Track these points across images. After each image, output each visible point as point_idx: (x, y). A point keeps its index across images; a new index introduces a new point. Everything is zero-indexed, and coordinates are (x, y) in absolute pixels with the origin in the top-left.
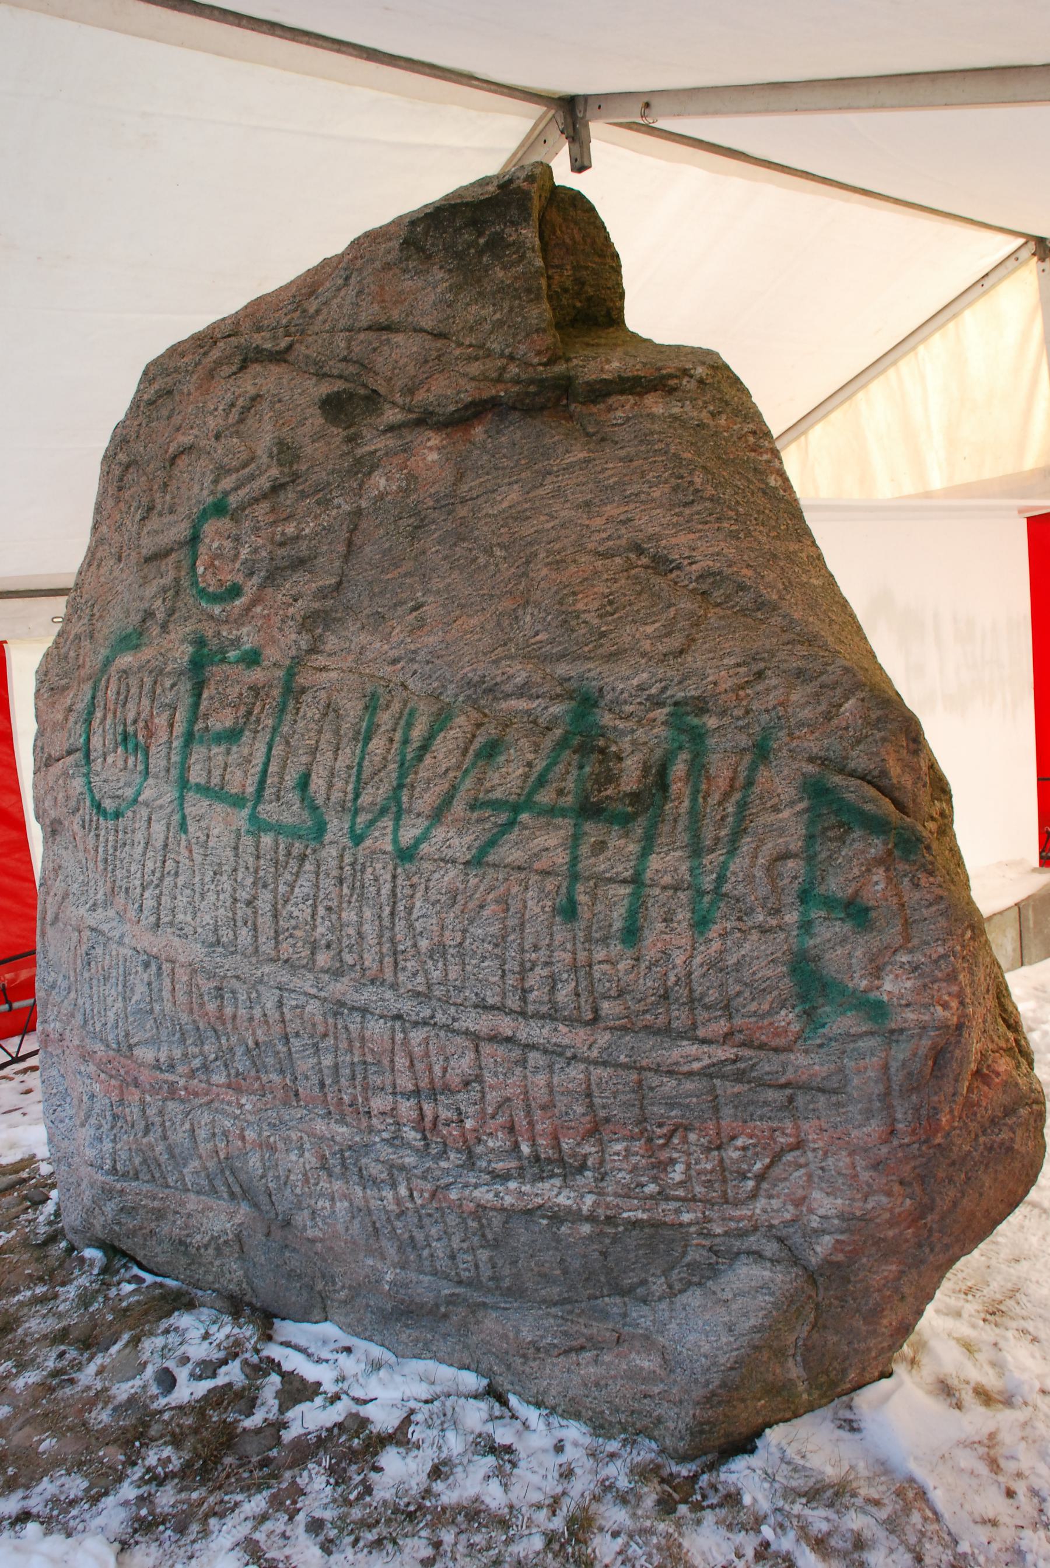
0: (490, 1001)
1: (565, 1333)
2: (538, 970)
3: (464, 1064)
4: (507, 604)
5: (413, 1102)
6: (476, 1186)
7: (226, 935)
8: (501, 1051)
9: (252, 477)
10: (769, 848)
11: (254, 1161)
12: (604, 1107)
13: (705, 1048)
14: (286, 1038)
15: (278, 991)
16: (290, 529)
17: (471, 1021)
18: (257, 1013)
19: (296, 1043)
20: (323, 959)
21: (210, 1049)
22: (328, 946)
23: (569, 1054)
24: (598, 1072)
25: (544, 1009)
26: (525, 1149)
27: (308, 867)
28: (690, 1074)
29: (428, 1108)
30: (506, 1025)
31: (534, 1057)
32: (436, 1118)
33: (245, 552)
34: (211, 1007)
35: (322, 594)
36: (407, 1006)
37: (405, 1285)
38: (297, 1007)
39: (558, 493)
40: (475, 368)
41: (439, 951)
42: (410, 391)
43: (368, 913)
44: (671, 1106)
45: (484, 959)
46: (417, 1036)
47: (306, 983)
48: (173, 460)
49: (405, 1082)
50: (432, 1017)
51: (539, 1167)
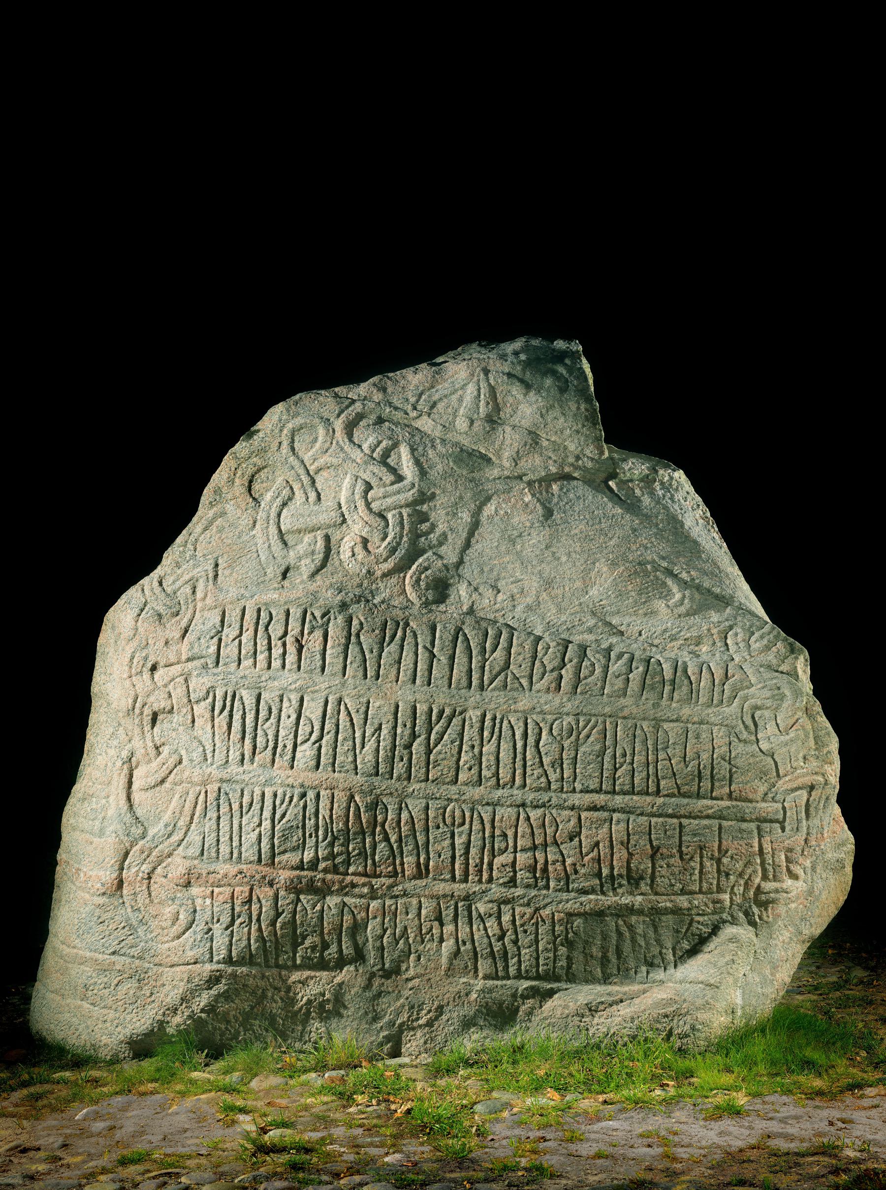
0: (592, 787)
1: (609, 994)
2: (624, 767)
5: (530, 854)
6: (567, 901)
12: (657, 839)
13: (715, 802)
15: (425, 801)
17: (575, 799)
22: (470, 769)
23: (638, 812)
24: (654, 820)
25: (626, 788)
26: (605, 872)
31: (616, 816)
32: (546, 861)
37: (490, 991)
38: (440, 808)
44: (695, 835)
45: (589, 764)
50: (549, 801)
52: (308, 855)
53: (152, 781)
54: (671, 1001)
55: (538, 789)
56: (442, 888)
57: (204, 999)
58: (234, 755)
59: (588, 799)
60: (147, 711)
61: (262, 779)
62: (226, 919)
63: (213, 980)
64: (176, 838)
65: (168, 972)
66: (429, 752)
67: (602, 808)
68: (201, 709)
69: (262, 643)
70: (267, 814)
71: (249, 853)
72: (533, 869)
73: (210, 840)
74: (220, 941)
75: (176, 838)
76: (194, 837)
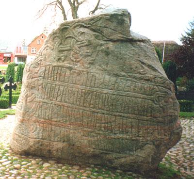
3: (114, 119)
4: (122, 65)
7: (75, 103)
8: (119, 117)
9: (83, 43)
10: (157, 95)
11: (71, 135)
14: (83, 117)
16: (88, 51)
18: (78, 113)
19: (84, 117)
20: (91, 106)
21: (67, 119)
24: (133, 120)
27: (91, 94)
28: (145, 120)
29: (106, 125)
30: (120, 114)
31: (124, 118)
33: (80, 53)
34: (70, 112)
35: (92, 60)
36: (105, 112)
39: (129, 53)
40: (119, 35)
41: (112, 105)
42: (109, 36)
43: (100, 100)
46: (106, 116)
47: (88, 109)
48: (67, 38)
49: (103, 121)
51: (122, 132)
52: (58, 119)
53: (30, 100)
54: (133, 160)
55: (107, 110)
56: (86, 129)
57: (37, 146)
58: (46, 97)
59: (118, 113)
60: (30, 87)
61: (50, 103)
62: (42, 130)
63: (38, 142)
64: (34, 112)
65: (31, 140)
66: (84, 100)
67: (121, 116)
68: (40, 87)
69: (52, 75)
70: (51, 110)
71: (47, 118)
72: (105, 127)
73: (40, 113)
74: (41, 135)
75: (34, 112)
76: (37, 113)
